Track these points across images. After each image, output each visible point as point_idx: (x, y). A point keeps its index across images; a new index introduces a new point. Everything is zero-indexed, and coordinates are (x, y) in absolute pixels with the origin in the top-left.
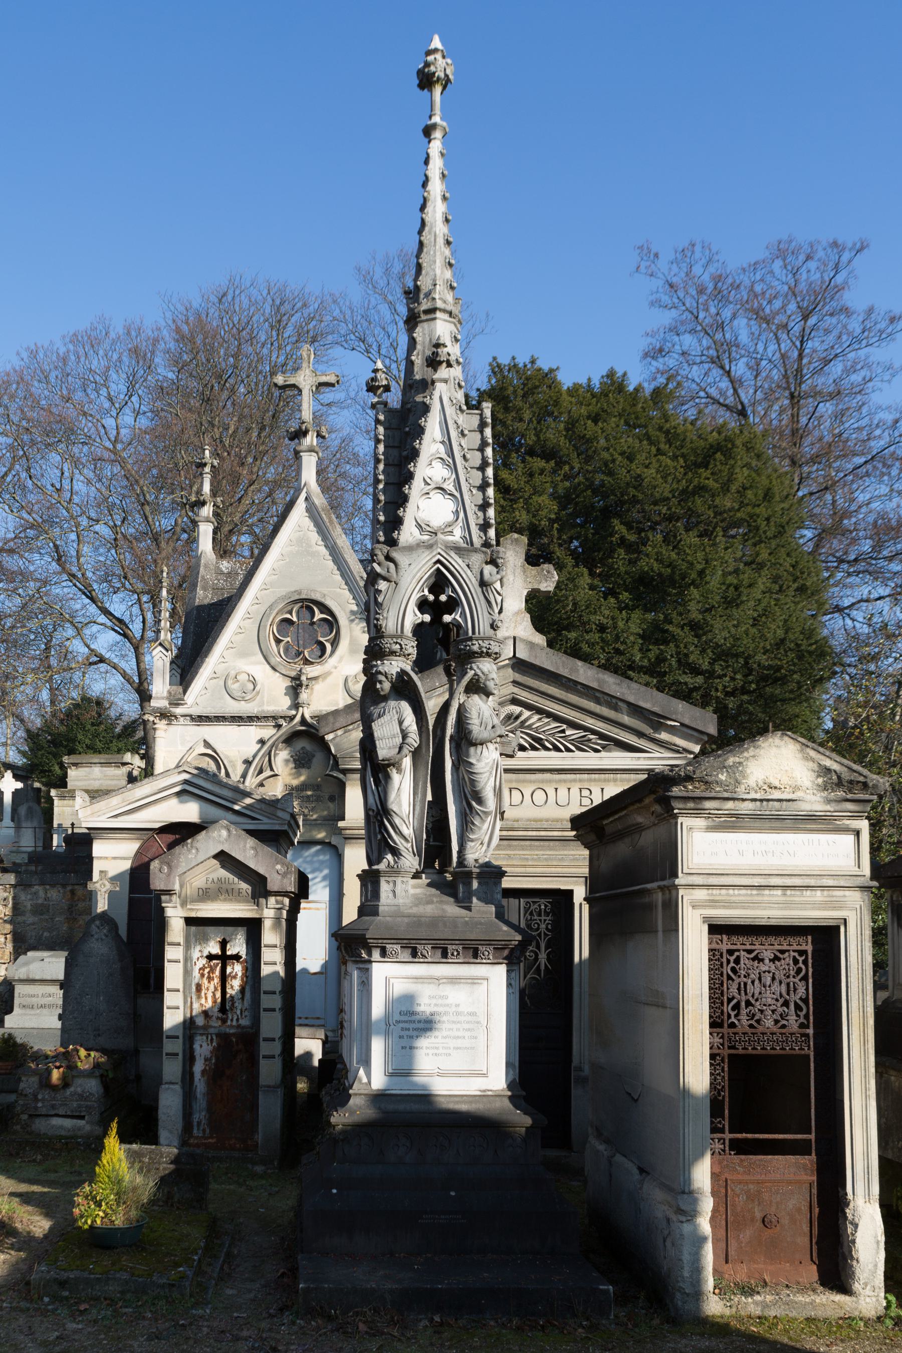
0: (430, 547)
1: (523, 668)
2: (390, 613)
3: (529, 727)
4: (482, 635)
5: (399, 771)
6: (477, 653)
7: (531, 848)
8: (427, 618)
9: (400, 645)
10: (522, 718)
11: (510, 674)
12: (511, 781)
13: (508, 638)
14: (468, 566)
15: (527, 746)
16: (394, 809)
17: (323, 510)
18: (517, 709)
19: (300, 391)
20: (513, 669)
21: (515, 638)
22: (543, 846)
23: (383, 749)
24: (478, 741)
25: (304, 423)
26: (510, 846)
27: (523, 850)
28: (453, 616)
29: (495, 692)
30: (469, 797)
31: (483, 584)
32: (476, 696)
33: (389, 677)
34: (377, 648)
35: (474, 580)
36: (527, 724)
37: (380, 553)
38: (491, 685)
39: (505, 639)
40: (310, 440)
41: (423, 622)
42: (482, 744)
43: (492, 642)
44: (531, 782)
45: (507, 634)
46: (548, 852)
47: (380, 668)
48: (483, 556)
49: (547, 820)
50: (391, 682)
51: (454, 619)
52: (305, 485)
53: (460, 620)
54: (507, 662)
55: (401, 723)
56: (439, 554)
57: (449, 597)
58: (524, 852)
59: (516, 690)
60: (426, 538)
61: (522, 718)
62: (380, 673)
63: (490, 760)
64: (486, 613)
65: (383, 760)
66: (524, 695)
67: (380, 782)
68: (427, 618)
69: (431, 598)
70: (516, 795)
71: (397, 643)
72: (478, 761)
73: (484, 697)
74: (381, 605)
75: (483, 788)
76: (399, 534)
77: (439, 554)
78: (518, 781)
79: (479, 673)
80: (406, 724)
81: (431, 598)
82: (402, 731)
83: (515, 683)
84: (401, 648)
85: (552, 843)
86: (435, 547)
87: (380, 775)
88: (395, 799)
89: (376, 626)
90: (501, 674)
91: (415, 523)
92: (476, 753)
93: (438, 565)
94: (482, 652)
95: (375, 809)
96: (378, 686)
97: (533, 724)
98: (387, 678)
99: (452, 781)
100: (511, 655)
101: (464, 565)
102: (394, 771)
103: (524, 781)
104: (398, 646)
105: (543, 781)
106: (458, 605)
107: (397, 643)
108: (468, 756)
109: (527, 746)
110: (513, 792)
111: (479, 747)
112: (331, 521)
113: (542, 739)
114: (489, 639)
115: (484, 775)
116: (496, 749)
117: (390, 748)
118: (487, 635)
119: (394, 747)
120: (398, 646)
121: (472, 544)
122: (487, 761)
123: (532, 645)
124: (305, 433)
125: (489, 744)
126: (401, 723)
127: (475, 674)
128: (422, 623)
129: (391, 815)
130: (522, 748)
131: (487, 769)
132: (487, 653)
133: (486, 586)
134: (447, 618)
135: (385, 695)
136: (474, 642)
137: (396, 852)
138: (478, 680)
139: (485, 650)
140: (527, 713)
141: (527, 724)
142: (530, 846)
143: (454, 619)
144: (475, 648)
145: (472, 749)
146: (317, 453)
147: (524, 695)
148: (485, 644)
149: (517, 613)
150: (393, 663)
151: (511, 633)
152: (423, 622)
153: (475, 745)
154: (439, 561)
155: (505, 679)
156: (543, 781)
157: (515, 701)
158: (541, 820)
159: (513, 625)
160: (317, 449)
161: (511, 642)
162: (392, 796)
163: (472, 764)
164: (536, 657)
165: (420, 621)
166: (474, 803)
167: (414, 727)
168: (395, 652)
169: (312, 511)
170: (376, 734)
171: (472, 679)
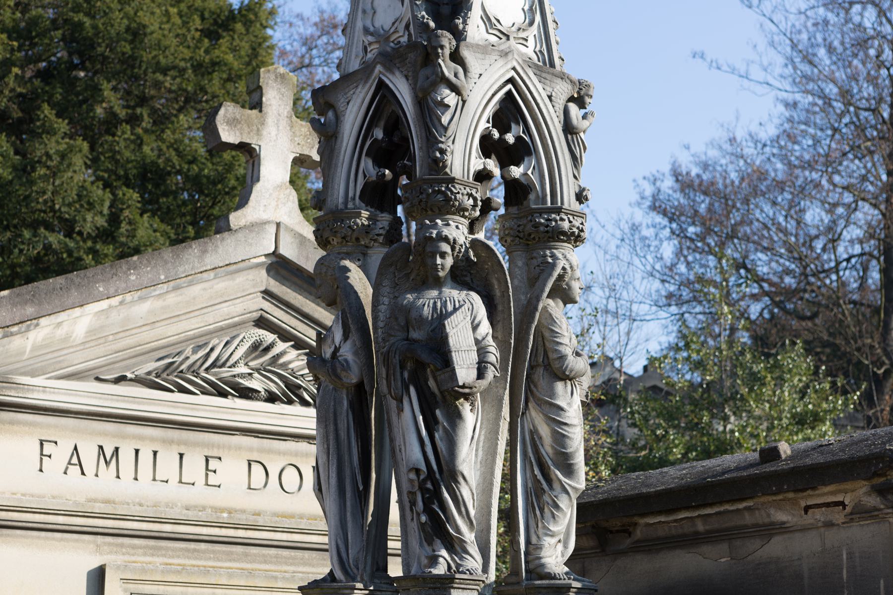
0: (505, 54)
1: (283, 272)
3: (284, 366)
4: (566, 206)
6: (564, 233)
7: (278, 560)
11: (263, 280)
12: (251, 449)
14: (550, 97)
16: (466, 473)
18: (270, 337)
20: (268, 271)
21: (278, 225)
22: (294, 558)
26: (246, 555)
27: (265, 562)
31: (569, 129)
34: (440, 197)
35: (556, 120)
36: (282, 361)
37: (447, 45)
44: (279, 453)
45: (265, 216)
46: (301, 569)
47: (446, 232)
48: (570, 87)
49: (301, 517)
51: (525, 174)
54: (263, 259)
56: (514, 69)
57: (518, 139)
58: (267, 567)
59: (267, 306)
60: (493, 39)
62: (446, 239)
65: (464, 387)
66: (278, 315)
67: (436, 422)
69: (496, 134)
70: (257, 469)
71: (470, 195)
74: (446, 129)
76: (465, 23)
77: (514, 69)
78: (261, 450)
81: (496, 134)
82: (477, 342)
83: (268, 294)
85: (307, 554)
86: (510, 57)
87: (438, 412)
89: (436, 161)
90: (251, 277)
91: (481, 13)
93: (510, 86)
95: (424, 468)
96: (439, 261)
97: (290, 362)
101: (544, 95)
103: (270, 451)
105: (296, 454)
106: (529, 154)
108: (553, 394)
110: (254, 465)
113: (300, 387)
118: (572, 208)
120: (471, 202)
121: (552, 65)
129: (457, 482)
130: (272, 398)
133: (571, 134)
137: (455, 546)
140: (281, 346)
141: (282, 361)
142: (276, 557)
144: (566, 225)
145: (559, 386)
147: (278, 315)
149: (280, 187)
154: (511, 81)
156: (296, 454)
157: (262, 323)
158: (292, 516)
159: (274, 203)
161: (272, 229)
163: (561, 409)
170: (452, 341)
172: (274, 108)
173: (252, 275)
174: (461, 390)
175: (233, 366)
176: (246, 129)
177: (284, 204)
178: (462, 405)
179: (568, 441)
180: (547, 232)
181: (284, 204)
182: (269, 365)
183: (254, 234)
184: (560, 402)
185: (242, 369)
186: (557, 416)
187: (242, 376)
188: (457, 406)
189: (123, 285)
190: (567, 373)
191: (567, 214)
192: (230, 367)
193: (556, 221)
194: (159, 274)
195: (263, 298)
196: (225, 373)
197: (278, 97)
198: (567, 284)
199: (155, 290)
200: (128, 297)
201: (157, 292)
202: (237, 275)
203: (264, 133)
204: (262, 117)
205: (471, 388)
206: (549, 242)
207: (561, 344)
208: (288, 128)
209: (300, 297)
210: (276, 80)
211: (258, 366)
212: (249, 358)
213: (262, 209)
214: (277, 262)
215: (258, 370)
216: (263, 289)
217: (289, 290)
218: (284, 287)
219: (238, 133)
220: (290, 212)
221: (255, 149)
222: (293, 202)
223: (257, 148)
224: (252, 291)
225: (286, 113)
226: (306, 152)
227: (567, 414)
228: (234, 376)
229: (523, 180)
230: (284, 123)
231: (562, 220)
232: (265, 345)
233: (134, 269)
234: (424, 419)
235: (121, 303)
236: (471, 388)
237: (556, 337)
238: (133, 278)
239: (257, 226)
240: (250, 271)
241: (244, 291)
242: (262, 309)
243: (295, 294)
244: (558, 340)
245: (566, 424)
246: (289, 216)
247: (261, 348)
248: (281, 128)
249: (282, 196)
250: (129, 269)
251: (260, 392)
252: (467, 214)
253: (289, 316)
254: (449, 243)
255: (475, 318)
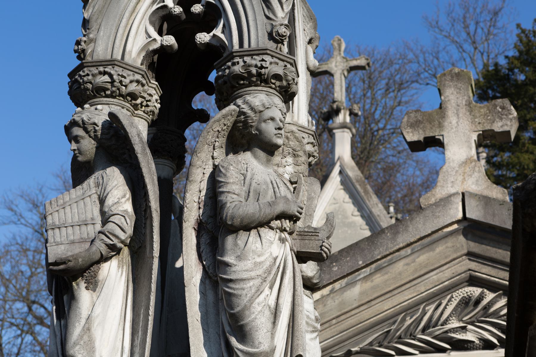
2: (101, 33)
3: (496, 314)
5: (93, 285)
6: (239, 77)
8: (170, 40)
9: (111, 76)
10: (485, 302)
11: (462, 243)
13: (454, 194)
15: (495, 341)
17: (358, 181)
18: (476, 291)
19: (332, 75)
20: (465, 236)
21: (463, 194)
23: (58, 244)
24: (237, 222)
25: (334, 102)
28: (211, 34)
29: (280, 141)
30: (227, 328)
32: (248, 154)
33: (90, 128)
36: (492, 310)
38: (269, 128)
39: (450, 196)
40: (343, 117)
41: (162, 46)
42: (248, 228)
43: (268, 58)
45: (453, 191)
50: (95, 138)
51: (214, 35)
52: (339, 159)
53: (222, 36)
54: (455, 226)
55: (102, 201)
59: (473, 265)
61: (485, 302)
63: (265, 259)
64: (261, 18)
68: (170, 40)
69: (178, 10)
72: (239, 258)
73: (261, 154)
75: (246, 308)
79: (246, 109)
80: (109, 201)
82: (103, 213)
83: (471, 255)
84: (113, 82)
87: (65, 298)
88: (81, 337)
90: (449, 244)
92: (236, 245)
94: (250, 73)
98: (87, 132)
99: (203, 306)
100: (460, 215)
102: (83, 285)
104: (106, 78)
107: (105, 73)
109: (495, 341)
111: (243, 235)
112: (366, 192)
114: (262, 52)
115: (251, 283)
116: (282, 241)
117: (73, 242)
119: (82, 241)
122: (258, 260)
123: (486, 201)
124: (337, 112)
125: (264, 231)
126: (102, 201)
127: (241, 113)
128: (163, 50)
131: (260, 272)
132: (259, 75)
134: (203, 37)
135: (88, 162)
136: (236, 60)
138: (245, 123)
139: (254, 71)
140: (490, 296)
141: (492, 310)
143: (214, 34)
144: (238, 69)
145: (230, 240)
146: (350, 129)
148: (256, 61)
150: (99, 107)
151: (458, 188)
152: (162, 46)
153: (234, 230)
155: (455, 251)
157: (473, 281)
159: (460, 178)
160: (350, 125)
162: (76, 331)
163: (227, 265)
164: (494, 215)
165: (156, 46)
166: (233, 341)
167: (128, 207)
168: (105, 89)
169: (346, 183)
171: (236, 123)
172: (453, 101)
173: (450, 242)
174: (55, 268)
175: (445, 323)
176: (428, 126)
177: (471, 176)
178: (78, 285)
179: (235, 300)
180: (225, 82)
181: (471, 176)
182: (482, 317)
183: (441, 208)
184: (229, 259)
185: (455, 324)
186: (224, 275)
187: (454, 330)
188: (72, 286)
189: (328, 277)
190: (230, 223)
191: (241, 57)
192: (442, 325)
193: (229, 68)
194: (358, 261)
195: (470, 260)
196: (439, 330)
197: (455, 93)
198: (257, 129)
199: (359, 275)
200: (337, 285)
201: (362, 276)
202: (434, 245)
203: (446, 124)
204: (442, 112)
205: (64, 263)
206: (235, 91)
207: (223, 192)
208: (468, 113)
209: (500, 251)
210: (452, 80)
211: (472, 319)
212: (463, 314)
213: (450, 185)
214: (468, 226)
215: (472, 324)
216: (465, 251)
217: (489, 248)
218: (484, 246)
219: (421, 131)
220: (477, 181)
221: (439, 139)
222: (479, 172)
223: (441, 138)
224: (455, 256)
225: (464, 103)
226: (488, 127)
227: (233, 269)
228: (446, 332)
229: (214, 43)
230: (463, 110)
231: (234, 64)
232: (473, 299)
233: (336, 262)
234: (56, 309)
235: (332, 292)
236: (64, 263)
237: (220, 187)
238: (335, 269)
239: (447, 200)
240: (446, 239)
241: (446, 257)
242: (470, 270)
243: (494, 249)
244: (221, 190)
245: (231, 281)
246: (477, 184)
247: (472, 303)
248: (461, 115)
249: (468, 169)
250: (332, 263)
251: (474, 342)
252: (108, 92)
253: (497, 270)
254: (79, 126)
255: (105, 190)
